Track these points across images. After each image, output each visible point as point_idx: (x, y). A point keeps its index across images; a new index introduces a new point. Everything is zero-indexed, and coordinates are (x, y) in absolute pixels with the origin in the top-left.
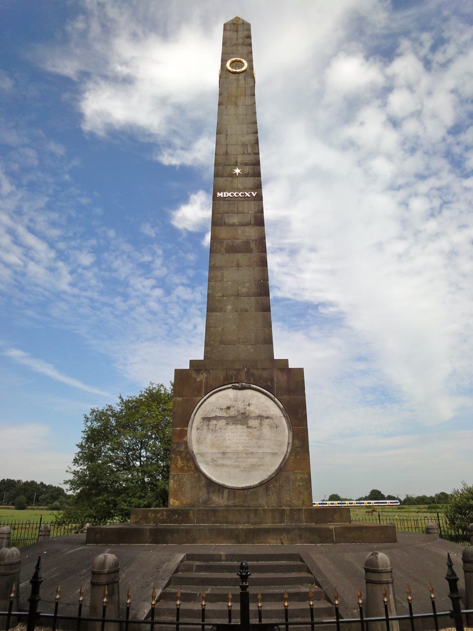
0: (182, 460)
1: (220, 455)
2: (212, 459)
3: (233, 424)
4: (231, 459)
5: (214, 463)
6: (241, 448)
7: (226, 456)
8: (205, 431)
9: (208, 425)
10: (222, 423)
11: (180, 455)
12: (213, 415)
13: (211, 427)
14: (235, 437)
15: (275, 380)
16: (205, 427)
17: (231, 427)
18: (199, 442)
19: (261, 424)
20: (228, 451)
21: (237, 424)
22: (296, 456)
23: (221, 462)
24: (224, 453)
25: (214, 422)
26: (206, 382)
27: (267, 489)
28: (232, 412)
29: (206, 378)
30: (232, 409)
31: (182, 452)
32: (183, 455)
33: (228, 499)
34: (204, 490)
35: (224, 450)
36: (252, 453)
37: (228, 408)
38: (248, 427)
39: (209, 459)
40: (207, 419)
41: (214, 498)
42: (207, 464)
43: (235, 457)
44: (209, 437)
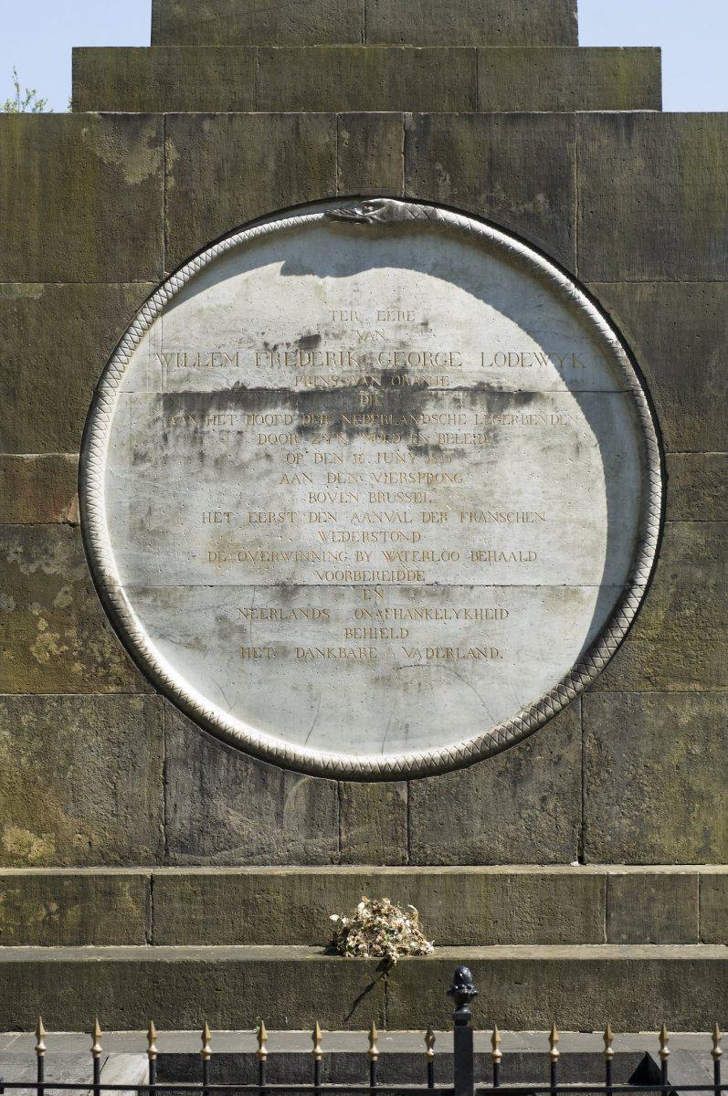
0: (58, 623)
1: (262, 600)
2: (221, 619)
3: (337, 429)
4: (322, 617)
5: (227, 641)
6: (377, 563)
7: (300, 602)
8: (177, 469)
9: (196, 438)
10: (280, 418)
11: (46, 601)
12: (223, 380)
13: (213, 447)
14: (343, 502)
15: (579, 180)
16: (179, 448)
17: (326, 446)
18: (143, 531)
19: (491, 436)
20: (308, 576)
21: (352, 433)
22: (676, 607)
23: (262, 635)
24: (286, 591)
25: (233, 418)
26: (184, 196)
27: (518, 778)
28: (329, 370)
29: (181, 172)
30: (324, 347)
31: (58, 581)
32: (62, 599)
33: (312, 823)
34: (183, 778)
35: (285, 569)
36: (442, 592)
37: (309, 342)
38: (419, 450)
39: (207, 622)
40: (188, 405)
41: (235, 819)
42: (192, 643)
43: (345, 607)
44: (205, 498)
